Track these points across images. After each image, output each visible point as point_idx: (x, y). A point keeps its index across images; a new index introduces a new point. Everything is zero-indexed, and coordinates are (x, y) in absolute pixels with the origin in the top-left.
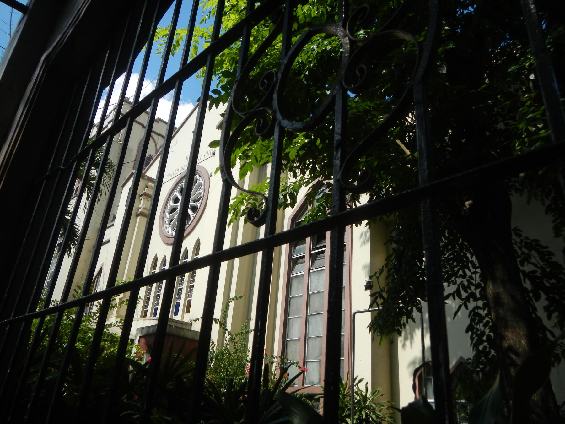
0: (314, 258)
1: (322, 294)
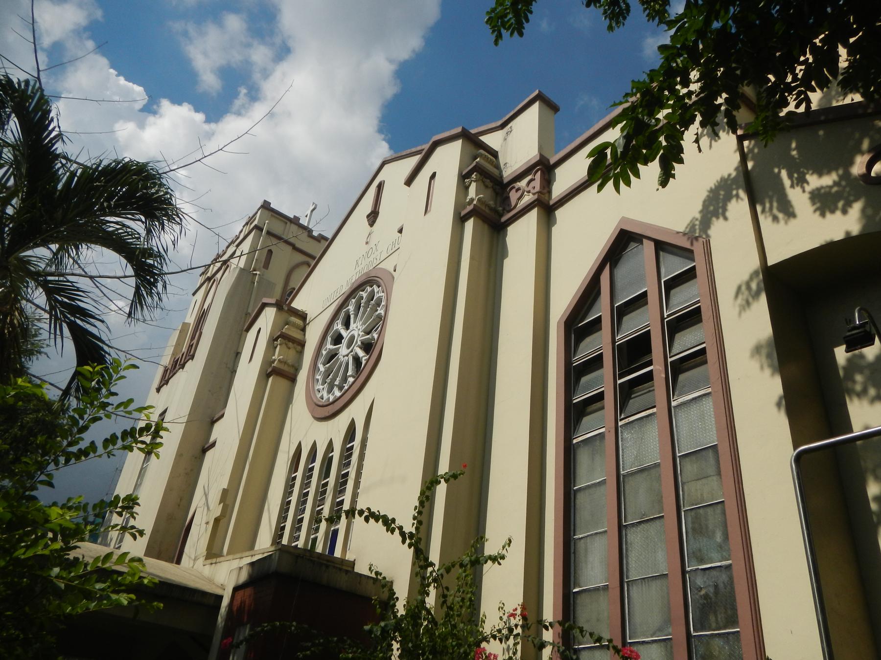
0: (625, 394)
1: (653, 471)
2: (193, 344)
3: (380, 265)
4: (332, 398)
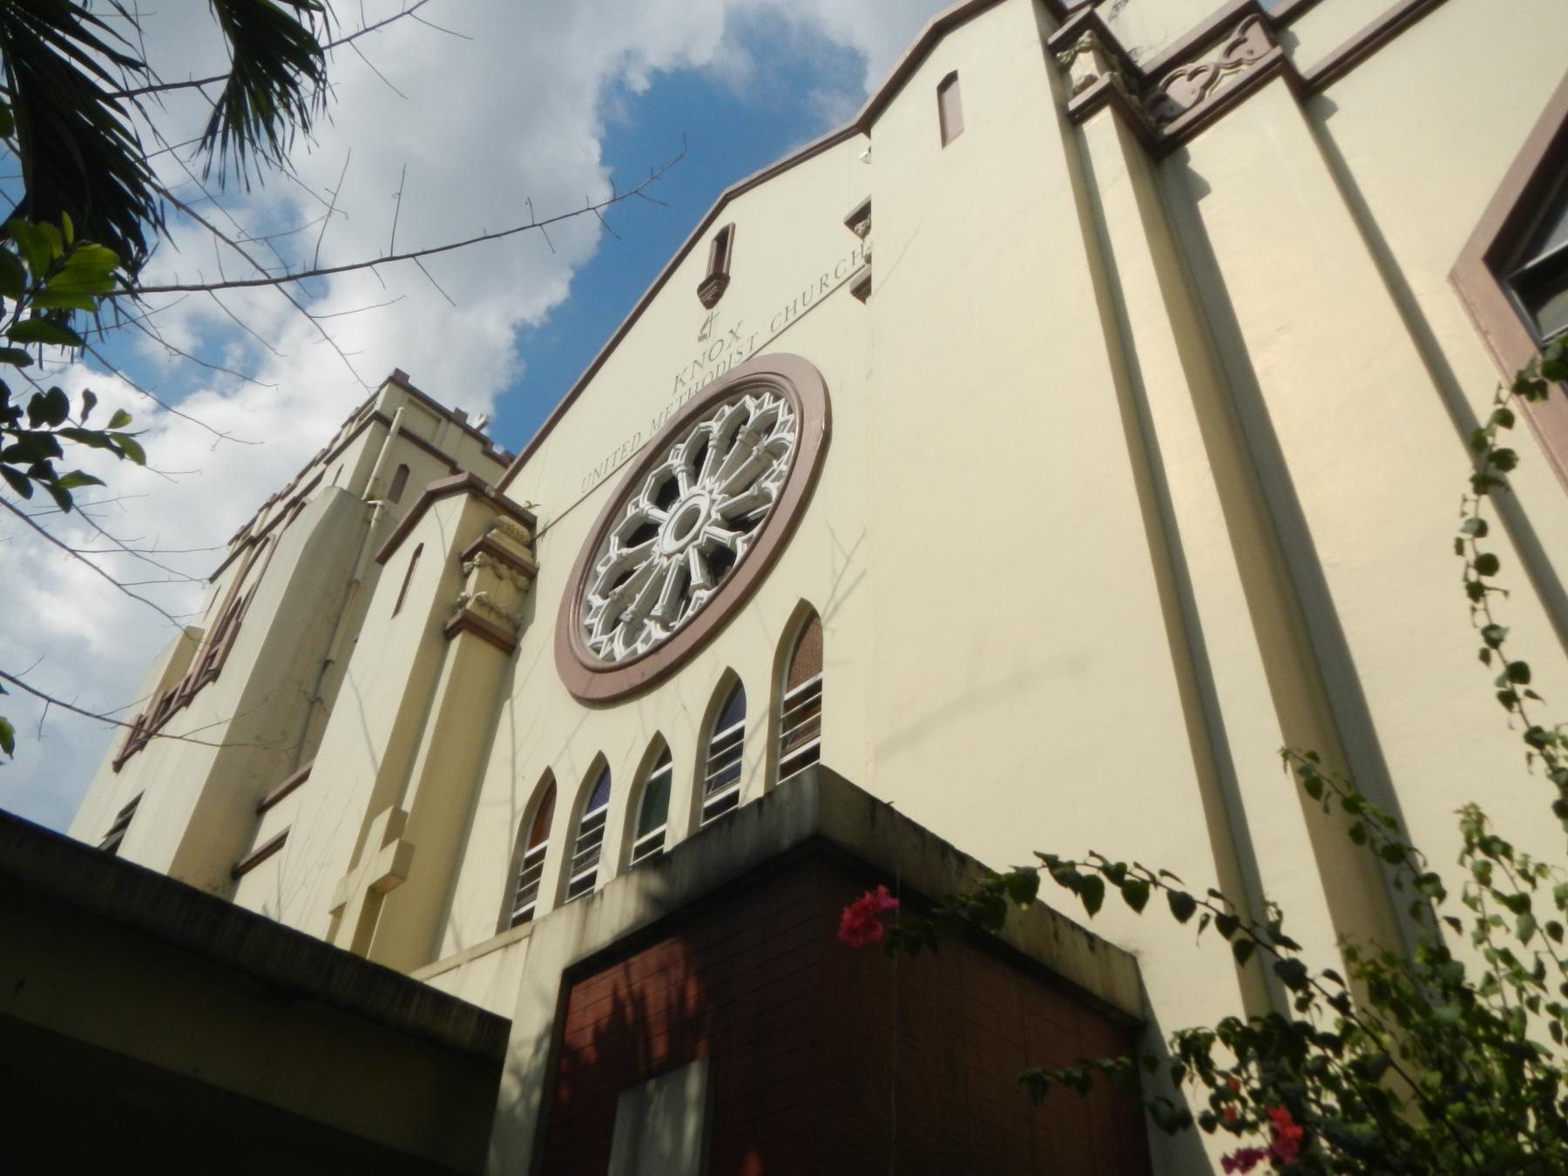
2: (216, 652)
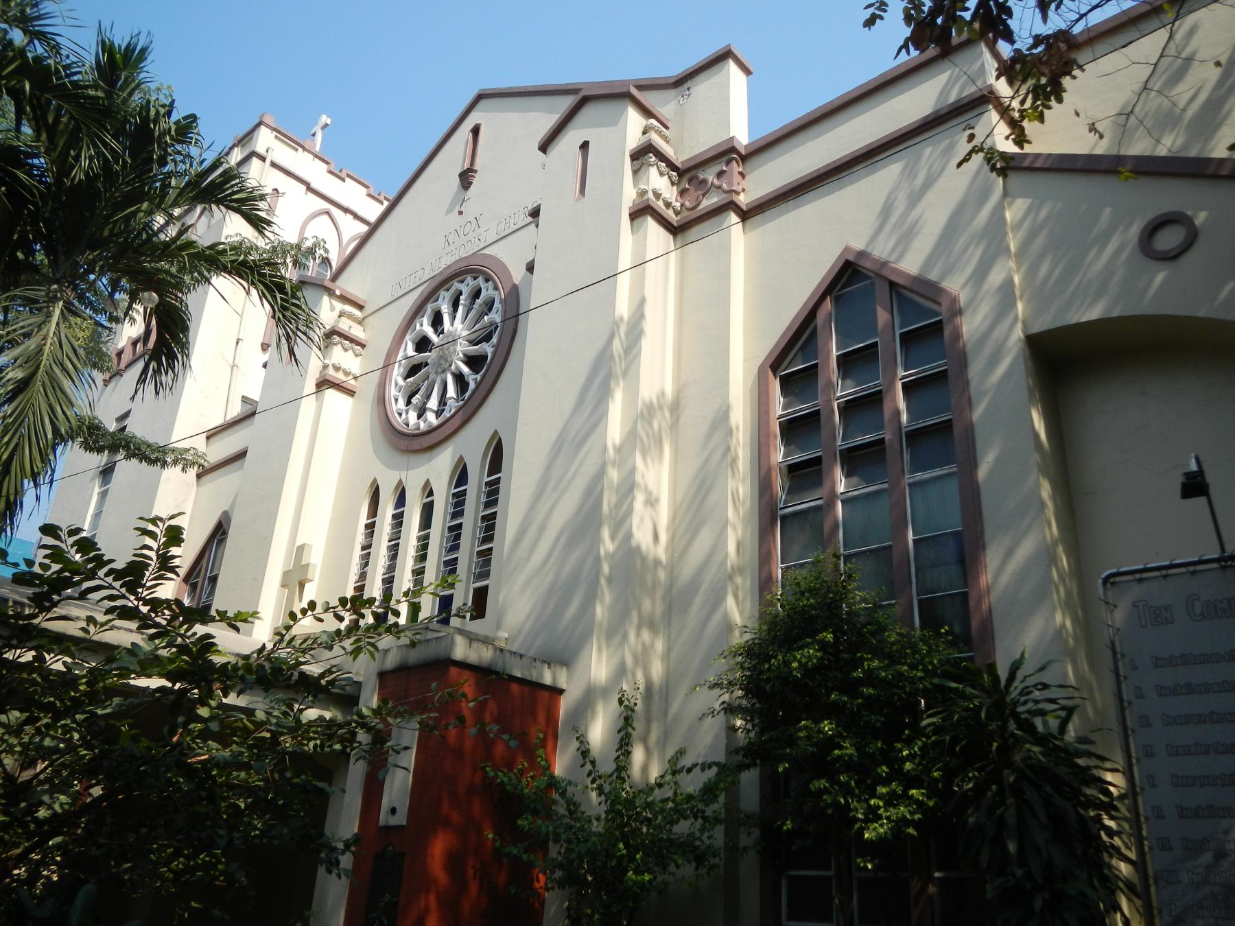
3: (491, 248)
4: (423, 426)
